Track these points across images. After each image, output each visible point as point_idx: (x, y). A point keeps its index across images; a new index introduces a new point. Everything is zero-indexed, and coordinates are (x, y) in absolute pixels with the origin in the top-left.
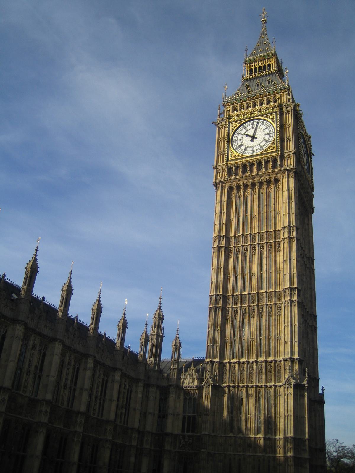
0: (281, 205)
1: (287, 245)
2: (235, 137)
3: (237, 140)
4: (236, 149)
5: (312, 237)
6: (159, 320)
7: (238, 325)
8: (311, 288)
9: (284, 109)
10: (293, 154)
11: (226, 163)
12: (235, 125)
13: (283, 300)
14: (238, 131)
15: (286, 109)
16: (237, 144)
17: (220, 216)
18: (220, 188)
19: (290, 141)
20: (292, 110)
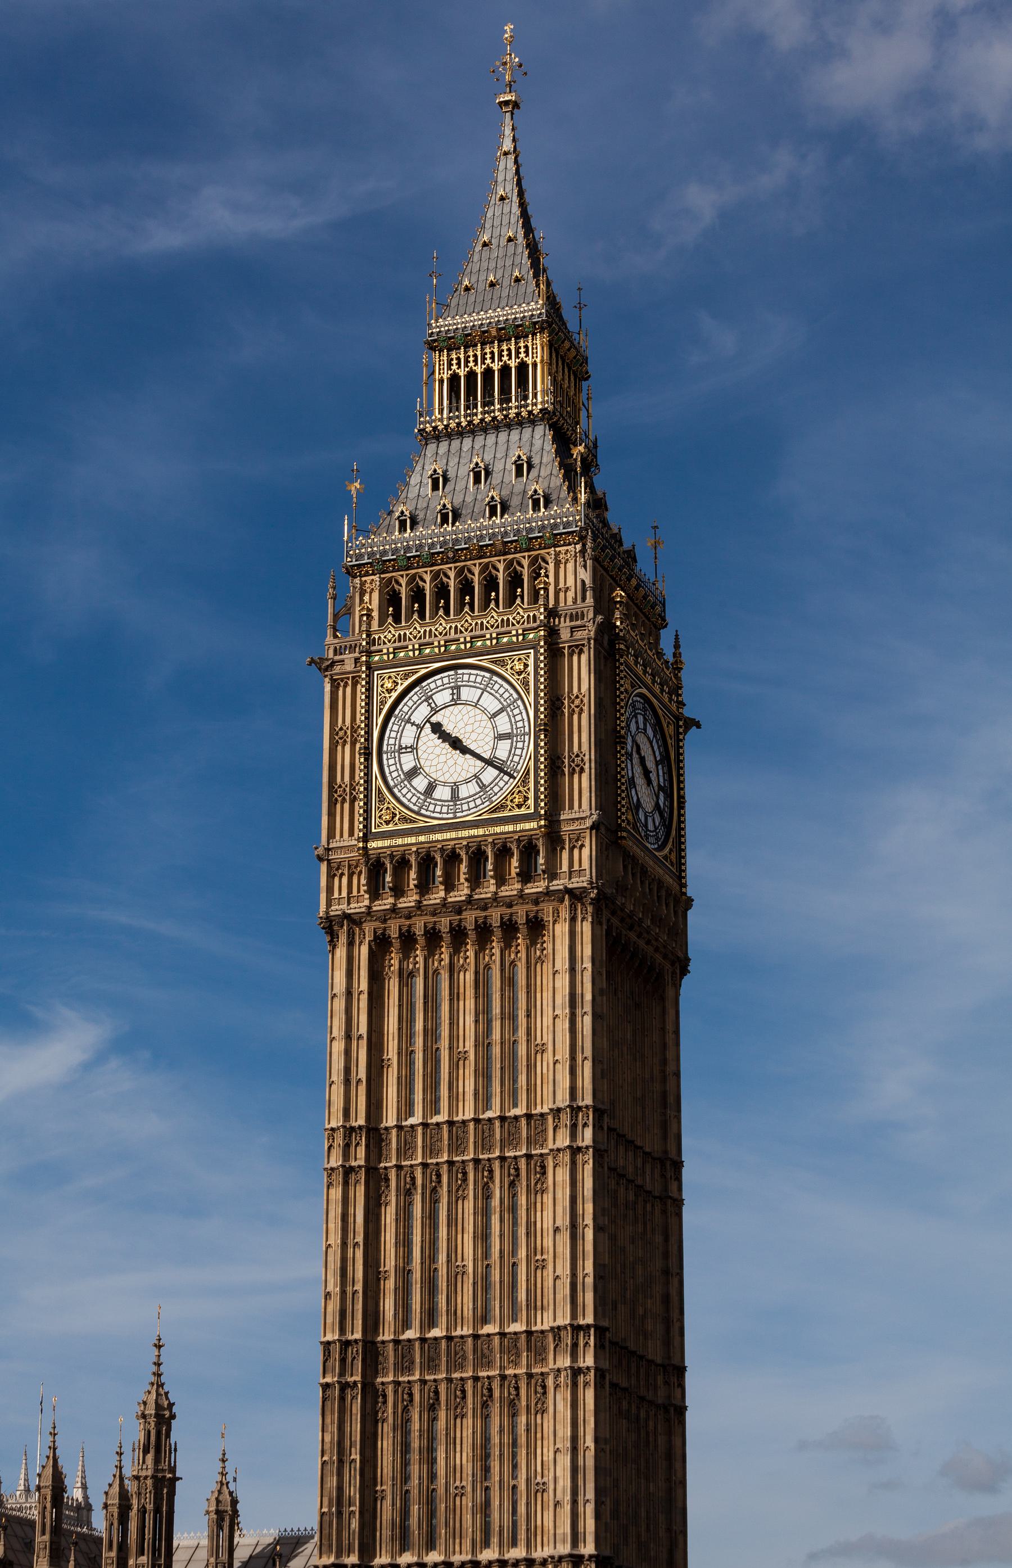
0: (548, 1020)
1: (563, 1175)
2: (393, 734)
3: (401, 747)
4: (396, 786)
5: (677, 1074)
6: (158, 1424)
7: (415, 1444)
8: (666, 1272)
9: (565, 635)
10: (592, 828)
11: (361, 845)
12: (389, 685)
13: (551, 1366)
14: (403, 708)
15: (572, 632)
16: (401, 765)
17: (348, 1052)
18: (343, 939)
19: (582, 770)
20: (592, 642)
